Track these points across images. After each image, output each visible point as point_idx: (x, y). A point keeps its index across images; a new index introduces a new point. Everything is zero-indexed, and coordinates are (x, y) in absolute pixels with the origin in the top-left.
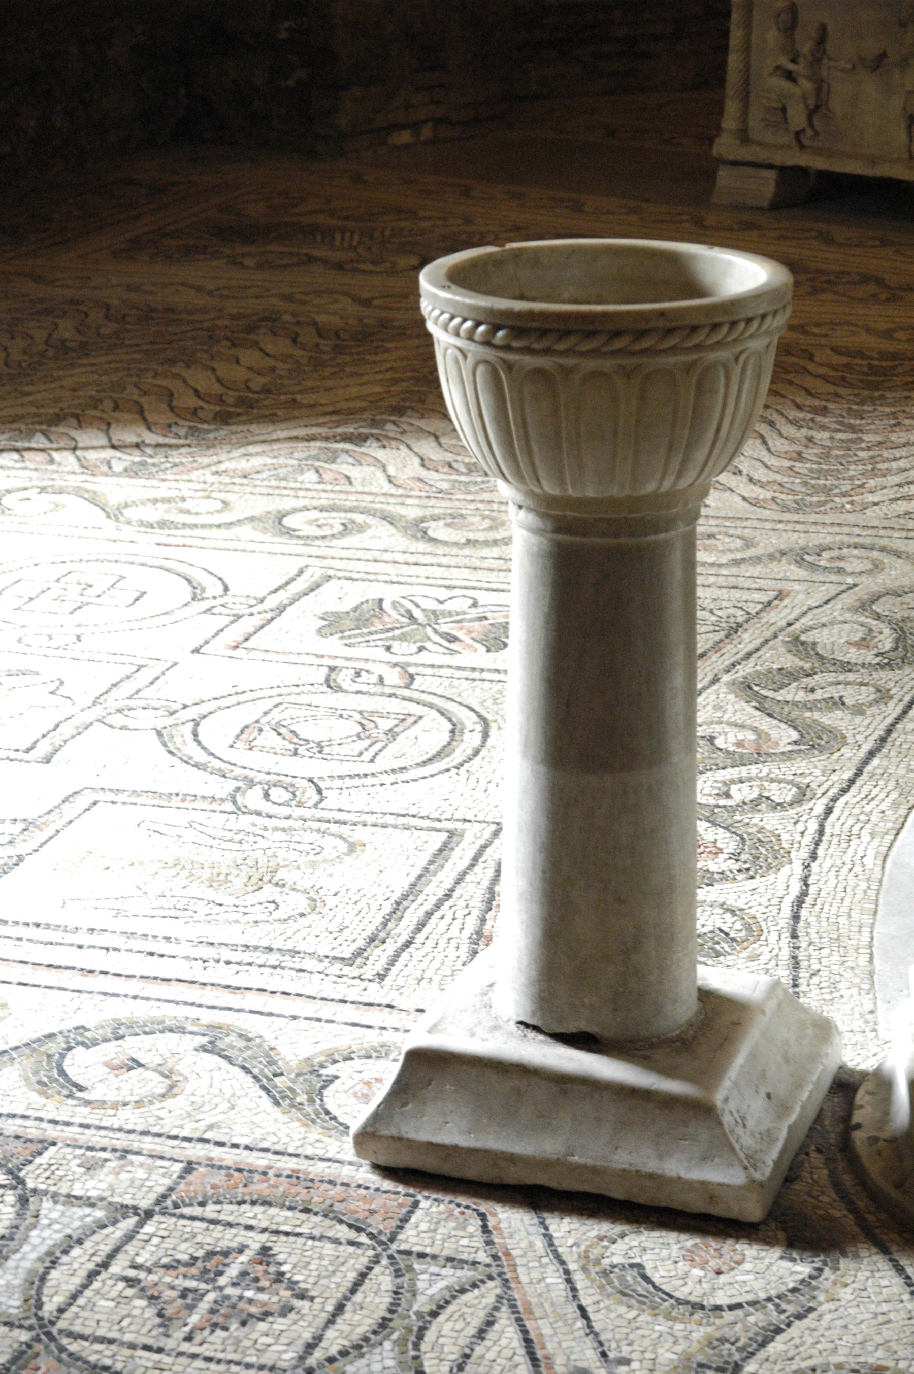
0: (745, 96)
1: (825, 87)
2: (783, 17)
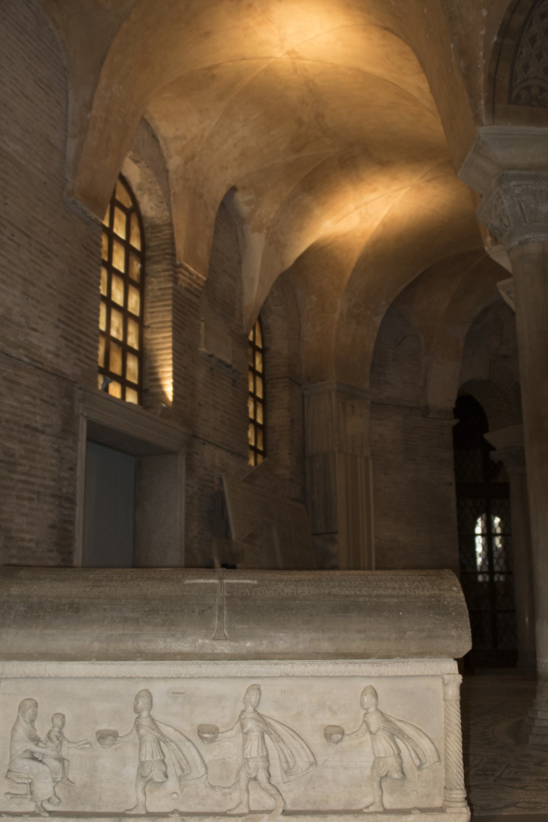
1: (66, 763)
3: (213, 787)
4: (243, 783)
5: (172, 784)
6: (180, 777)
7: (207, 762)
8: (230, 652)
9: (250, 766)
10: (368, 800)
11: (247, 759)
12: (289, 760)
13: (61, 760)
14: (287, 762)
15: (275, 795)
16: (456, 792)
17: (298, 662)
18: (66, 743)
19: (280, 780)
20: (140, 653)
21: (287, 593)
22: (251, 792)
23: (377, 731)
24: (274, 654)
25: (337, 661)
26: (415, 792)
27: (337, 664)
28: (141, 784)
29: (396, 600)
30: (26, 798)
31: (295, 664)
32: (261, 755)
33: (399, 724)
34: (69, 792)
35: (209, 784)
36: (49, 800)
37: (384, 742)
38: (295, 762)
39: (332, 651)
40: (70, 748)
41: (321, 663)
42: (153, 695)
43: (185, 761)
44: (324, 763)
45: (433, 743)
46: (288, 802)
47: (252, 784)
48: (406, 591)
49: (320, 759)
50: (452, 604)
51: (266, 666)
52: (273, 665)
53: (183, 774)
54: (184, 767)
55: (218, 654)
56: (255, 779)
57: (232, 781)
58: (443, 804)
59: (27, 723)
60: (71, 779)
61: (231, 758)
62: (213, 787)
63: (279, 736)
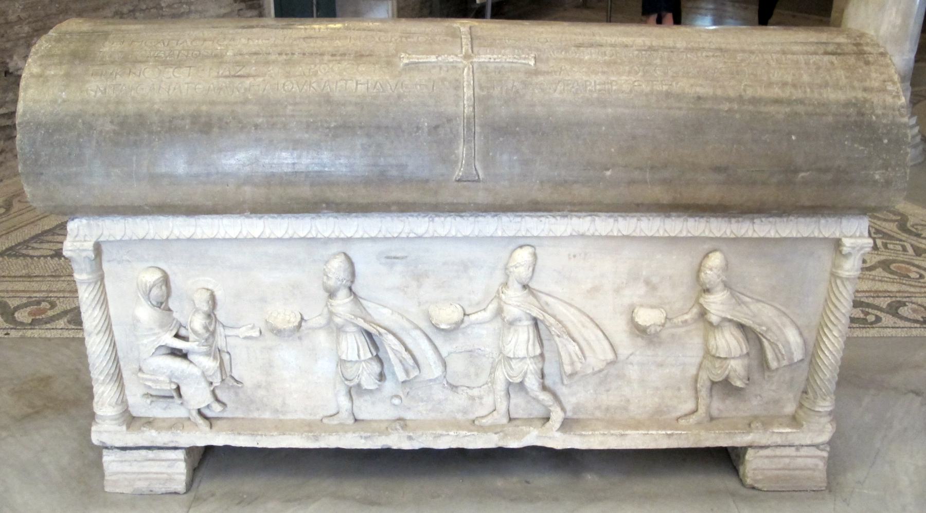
0: (118, 377)
1: (226, 357)
3: (454, 387)
4: (500, 386)
5: (389, 386)
6: (403, 382)
7: (444, 354)
9: (513, 367)
11: (510, 358)
13: (217, 353)
14: (572, 363)
18: (222, 329)
19: (557, 379)
21: (591, 91)
22: (512, 396)
26: (759, 398)
27: (669, 216)
28: (343, 391)
29: (788, 110)
31: (595, 215)
32: (532, 354)
34: (237, 394)
35: (447, 382)
37: (727, 335)
39: (665, 202)
40: (229, 336)
41: (642, 216)
42: (354, 260)
45: (801, 334)
46: (568, 408)
48: (805, 92)
49: (623, 352)
51: (547, 220)
52: (558, 218)
53: (408, 379)
54: (410, 368)
57: (484, 377)
59: (154, 306)
60: (236, 377)
61: (482, 351)
62: (454, 387)
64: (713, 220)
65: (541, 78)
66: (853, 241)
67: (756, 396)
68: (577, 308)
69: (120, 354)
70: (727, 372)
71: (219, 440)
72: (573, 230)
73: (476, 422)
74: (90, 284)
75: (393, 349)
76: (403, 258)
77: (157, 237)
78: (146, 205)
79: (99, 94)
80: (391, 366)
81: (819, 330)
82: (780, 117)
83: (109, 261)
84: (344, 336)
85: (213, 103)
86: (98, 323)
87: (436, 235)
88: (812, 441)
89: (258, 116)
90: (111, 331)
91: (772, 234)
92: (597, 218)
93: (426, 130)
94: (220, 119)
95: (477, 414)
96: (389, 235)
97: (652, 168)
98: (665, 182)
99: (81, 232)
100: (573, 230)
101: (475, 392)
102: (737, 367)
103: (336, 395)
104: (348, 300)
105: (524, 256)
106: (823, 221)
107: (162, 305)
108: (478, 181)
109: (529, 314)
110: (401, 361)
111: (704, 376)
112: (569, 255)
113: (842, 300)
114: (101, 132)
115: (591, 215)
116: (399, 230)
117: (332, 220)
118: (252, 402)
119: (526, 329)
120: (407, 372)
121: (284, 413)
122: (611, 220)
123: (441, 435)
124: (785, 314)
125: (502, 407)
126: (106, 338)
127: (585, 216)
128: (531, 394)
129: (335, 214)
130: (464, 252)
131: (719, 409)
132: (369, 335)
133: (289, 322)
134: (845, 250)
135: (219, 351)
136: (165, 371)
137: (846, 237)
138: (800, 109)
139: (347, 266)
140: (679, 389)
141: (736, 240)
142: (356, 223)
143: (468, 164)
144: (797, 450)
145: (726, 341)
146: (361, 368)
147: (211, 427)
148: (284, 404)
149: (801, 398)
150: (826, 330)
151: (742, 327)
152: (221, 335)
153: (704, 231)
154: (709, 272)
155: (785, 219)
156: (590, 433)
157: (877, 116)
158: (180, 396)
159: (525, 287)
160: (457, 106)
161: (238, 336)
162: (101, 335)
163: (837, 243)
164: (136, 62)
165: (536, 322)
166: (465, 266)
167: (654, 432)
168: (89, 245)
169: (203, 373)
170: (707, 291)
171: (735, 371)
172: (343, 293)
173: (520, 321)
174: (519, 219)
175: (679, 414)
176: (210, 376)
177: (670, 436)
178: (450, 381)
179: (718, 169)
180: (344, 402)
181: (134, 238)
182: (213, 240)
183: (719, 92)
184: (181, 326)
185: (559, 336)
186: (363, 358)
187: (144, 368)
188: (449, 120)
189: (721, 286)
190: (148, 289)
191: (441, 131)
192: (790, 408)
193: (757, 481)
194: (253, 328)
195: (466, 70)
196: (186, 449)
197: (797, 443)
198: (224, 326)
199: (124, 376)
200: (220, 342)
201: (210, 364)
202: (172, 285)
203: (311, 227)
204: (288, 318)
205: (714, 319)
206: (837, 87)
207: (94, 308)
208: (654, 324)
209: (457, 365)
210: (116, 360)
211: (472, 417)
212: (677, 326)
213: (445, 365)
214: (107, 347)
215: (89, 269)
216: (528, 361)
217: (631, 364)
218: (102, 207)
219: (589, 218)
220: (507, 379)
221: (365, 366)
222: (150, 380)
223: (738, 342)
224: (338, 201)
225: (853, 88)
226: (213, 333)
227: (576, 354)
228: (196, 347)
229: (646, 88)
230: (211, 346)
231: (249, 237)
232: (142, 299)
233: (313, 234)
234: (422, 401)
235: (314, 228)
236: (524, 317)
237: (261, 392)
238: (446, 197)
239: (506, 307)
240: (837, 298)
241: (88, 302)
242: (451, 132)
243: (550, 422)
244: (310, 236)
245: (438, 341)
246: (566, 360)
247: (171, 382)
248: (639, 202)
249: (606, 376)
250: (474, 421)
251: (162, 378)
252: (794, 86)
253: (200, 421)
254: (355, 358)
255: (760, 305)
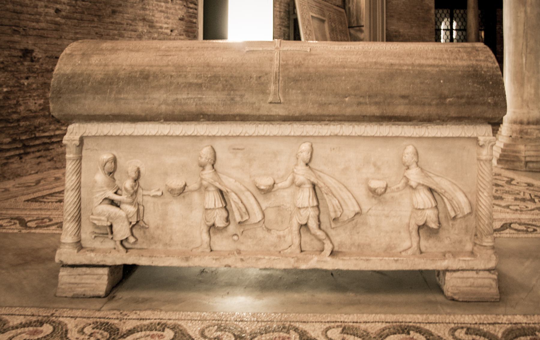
0: (78, 219)
1: (141, 208)
2: (108, 165)
4: (295, 228)
5: (232, 228)
6: (239, 223)
7: (264, 208)
8: (284, 114)
10: (407, 244)
11: (299, 208)
12: (337, 209)
14: (335, 212)
15: (324, 239)
16: (486, 240)
17: (347, 124)
18: (141, 191)
19: (328, 225)
20: (203, 115)
22: (302, 235)
23: (417, 186)
24: (324, 116)
25: (382, 123)
26: (448, 239)
27: (382, 125)
29: (437, 69)
30: (107, 237)
32: (311, 205)
33: (437, 179)
34: (144, 233)
35: (265, 227)
36: (127, 239)
37: (422, 194)
38: (342, 211)
39: (378, 115)
40: (145, 195)
42: (216, 150)
43: (244, 210)
44: (368, 212)
45: (466, 196)
46: (336, 244)
47: (303, 230)
49: (365, 208)
50: (489, 74)
52: (323, 126)
53: (242, 221)
55: (273, 116)
56: (306, 225)
58: (473, 249)
62: (269, 230)
63: (328, 188)
64: (405, 127)
65: (312, 57)
66: (484, 138)
67: (447, 238)
68: (336, 180)
69: (82, 206)
70: (425, 218)
71: (130, 260)
72: (331, 132)
73: (282, 252)
74: (74, 160)
75: (234, 202)
76: (242, 149)
77: (114, 134)
78: (111, 115)
79: (97, 62)
80: (233, 212)
81: (477, 195)
82: (434, 72)
83: (86, 149)
84: (208, 193)
85: (152, 66)
86: (73, 184)
87: (259, 134)
88: (485, 266)
89: (173, 71)
90: (80, 191)
91: (439, 135)
92: (343, 126)
93: (255, 78)
94: (154, 73)
95: (282, 248)
96: (234, 135)
97: (369, 96)
98: (376, 103)
99: (75, 131)
100: (331, 132)
101: (281, 233)
102: (430, 215)
103: (201, 233)
104: (211, 171)
105: (305, 147)
106: (466, 127)
107: (111, 173)
108: (280, 103)
109: (309, 180)
110: (238, 209)
111: (413, 222)
112: (331, 149)
113: (485, 173)
114: (94, 78)
115: (340, 124)
116: (240, 132)
117: (205, 126)
118: (153, 238)
119: (308, 189)
120: (242, 217)
121: (170, 245)
122: (351, 127)
123: (260, 259)
124: (455, 184)
125: (296, 241)
126: (76, 194)
127: (337, 125)
128: (312, 232)
129: (208, 122)
130: (274, 146)
131: (425, 247)
132: (221, 192)
133: (178, 185)
134: (481, 143)
135: (138, 204)
136: (106, 213)
137: (480, 136)
138: (444, 68)
139: (212, 151)
140: (400, 232)
141: (421, 138)
142: (218, 127)
143: (275, 94)
144: (477, 273)
145: (422, 198)
146: (216, 213)
147: (127, 252)
148: (171, 239)
149: (474, 239)
150: (480, 193)
151: (431, 190)
152: (140, 194)
153: (401, 133)
154: (407, 155)
155: (445, 126)
156: (348, 258)
157: (485, 72)
158: (112, 233)
159: (307, 165)
160: (271, 68)
161: (149, 195)
162: (74, 191)
163: (476, 139)
164: (118, 50)
165: (314, 186)
166: (275, 154)
167: (387, 258)
168: (77, 137)
169: (127, 216)
170: (408, 168)
171: (430, 217)
172: (209, 167)
173: (305, 184)
174: (303, 126)
175: (401, 249)
176: (131, 218)
177: (397, 261)
178: (267, 226)
179: (403, 97)
180: (205, 237)
181: (102, 134)
182: (143, 136)
183: (402, 62)
184: (119, 189)
185: (326, 194)
186: (217, 206)
187: (94, 212)
188: (266, 74)
189: (414, 165)
190: (104, 163)
191: (262, 79)
192: (469, 247)
193: (455, 294)
194: (159, 190)
195: (276, 53)
196: (110, 267)
197: (476, 268)
198: (142, 189)
199: (82, 220)
200: (139, 199)
201: (132, 209)
202: (118, 165)
203: (194, 130)
204: (178, 184)
205: (413, 183)
206: (462, 59)
207: (73, 175)
208: (380, 188)
209: (271, 215)
210: (80, 209)
211: (279, 249)
212: (393, 191)
213: (264, 215)
214: (76, 200)
215: (74, 152)
216: (310, 209)
217: (370, 215)
218: (88, 115)
219: (339, 126)
220: (299, 223)
221: (218, 212)
222: (96, 220)
223: (429, 199)
224: (209, 113)
225: (470, 60)
226: (136, 192)
227: (337, 206)
228: (125, 199)
229: (365, 60)
230: (134, 200)
231: (162, 134)
232: (100, 170)
233: (195, 133)
234: (251, 238)
235: (196, 130)
236: (306, 182)
237: (159, 232)
238: (264, 112)
239: (297, 176)
240: (482, 172)
241: (71, 171)
242: (268, 80)
243: (324, 251)
244: (193, 134)
245: (260, 200)
246: (331, 209)
247: (108, 221)
248: (364, 114)
249: (356, 224)
250: (280, 252)
251: (103, 218)
252: (440, 59)
253: (121, 248)
254: (212, 206)
255: (439, 179)
